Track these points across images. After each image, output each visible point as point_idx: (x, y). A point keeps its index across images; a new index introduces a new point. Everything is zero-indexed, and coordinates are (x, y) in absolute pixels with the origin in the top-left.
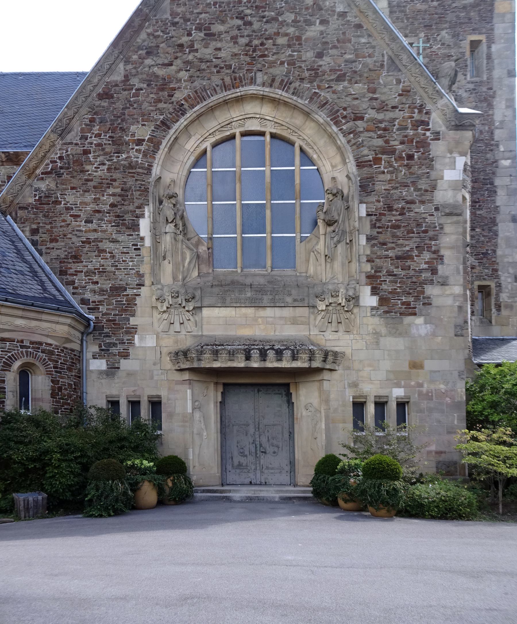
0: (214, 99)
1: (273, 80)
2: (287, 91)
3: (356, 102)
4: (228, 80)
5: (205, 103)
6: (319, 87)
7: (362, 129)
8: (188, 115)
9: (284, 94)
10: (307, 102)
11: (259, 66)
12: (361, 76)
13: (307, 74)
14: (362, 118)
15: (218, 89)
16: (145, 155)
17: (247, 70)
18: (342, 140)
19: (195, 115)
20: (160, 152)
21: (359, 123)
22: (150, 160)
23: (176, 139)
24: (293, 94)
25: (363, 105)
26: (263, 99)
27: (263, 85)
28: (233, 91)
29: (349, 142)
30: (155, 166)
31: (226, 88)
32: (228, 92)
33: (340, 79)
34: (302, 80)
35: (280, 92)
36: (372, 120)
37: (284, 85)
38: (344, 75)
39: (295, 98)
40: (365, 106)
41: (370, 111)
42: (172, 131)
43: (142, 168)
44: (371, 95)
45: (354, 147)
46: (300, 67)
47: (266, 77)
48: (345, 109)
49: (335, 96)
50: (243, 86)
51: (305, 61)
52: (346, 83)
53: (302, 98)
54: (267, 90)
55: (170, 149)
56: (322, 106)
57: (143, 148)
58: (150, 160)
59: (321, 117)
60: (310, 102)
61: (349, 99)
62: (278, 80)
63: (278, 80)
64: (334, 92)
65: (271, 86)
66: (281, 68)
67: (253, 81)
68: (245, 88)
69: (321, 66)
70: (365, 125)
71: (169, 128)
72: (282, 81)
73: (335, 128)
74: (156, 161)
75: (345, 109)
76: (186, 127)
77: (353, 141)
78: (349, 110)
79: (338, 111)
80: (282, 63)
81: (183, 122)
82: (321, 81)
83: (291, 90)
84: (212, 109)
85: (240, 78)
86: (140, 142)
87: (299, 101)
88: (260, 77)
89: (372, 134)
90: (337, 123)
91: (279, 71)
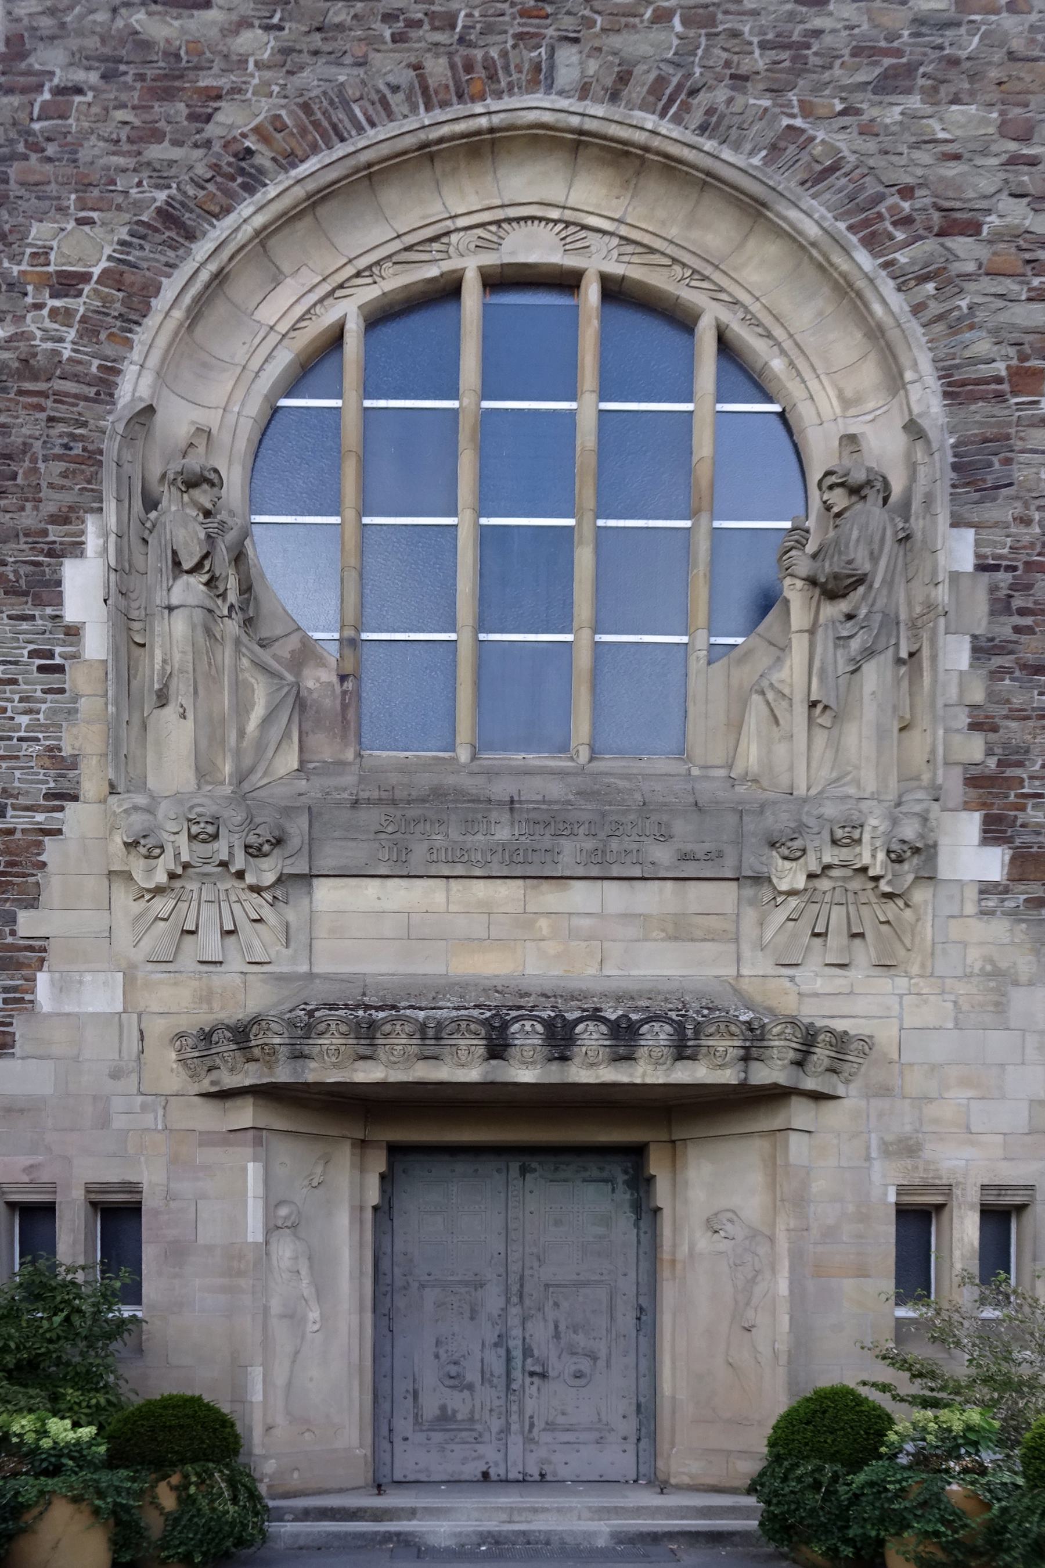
0: (378, 138)
1: (624, 78)
2: (677, 120)
3: (952, 170)
4: (437, 69)
5: (341, 150)
6: (807, 110)
7: (970, 267)
8: (272, 191)
9: (665, 127)
10: (756, 161)
11: (568, 23)
12: (973, 77)
13: (759, 61)
14: (972, 229)
15: (396, 100)
16: (89, 330)
17: (520, 37)
18: (890, 302)
19: (299, 192)
20: (152, 322)
21: (960, 244)
22: (109, 350)
23: (220, 278)
24: (703, 129)
25: (980, 181)
26: (576, 146)
27: (584, 91)
28: (458, 109)
29: (917, 309)
30: (130, 371)
31: (429, 97)
32: (439, 115)
33: (891, 83)
34: (740, 80)
35: (650, 121)
36: (1015, 236)
37: (665, 97)
38: (910, 69)
39: (709, 145)
40: (986, 184)
41: (1006, 203)
42: (202, 249)
43: (76, 378)
44: (1012, 146)
45: (939, 328)
46: (735, 34)
47: (593, 66)
48: (907, 192)
49: (871, 145)
50: (499, 95)
51: (755, 13)
52: (914, 102)
53: (737, 147)
54: (599, 110)
55: (196, 314)
56: (819, 177)
57: (79, 305)
58: (109, 350)
59: (812, 216)
60: (767, 161)
61: (924, 156)
62: (644, 78)
63: (644, 78)
64: (867, 131)
65: (614, 97)
66: (657, 35)
67: (541, 77)
68: (508, 102)
69: (818, 33)
70: (983, 252)
71: (191, 236)
72: (661, 81)
73: (864, 258)
74: (136, 355)
75: (907, 192)
76: (263, 237)
77: (935, 308)
78: (924, 199)
79: (880, 198)
80: (662, 17)
81: (248, 215)
82: (817, 88)
83: (697, 118)
84: (370, 178)
85: (489, 65)
86: (68, 283)
87: (727, 154)
88: (569, 63)
89: (1010, 286)
90: (872, 242)
91: (649, 46)
